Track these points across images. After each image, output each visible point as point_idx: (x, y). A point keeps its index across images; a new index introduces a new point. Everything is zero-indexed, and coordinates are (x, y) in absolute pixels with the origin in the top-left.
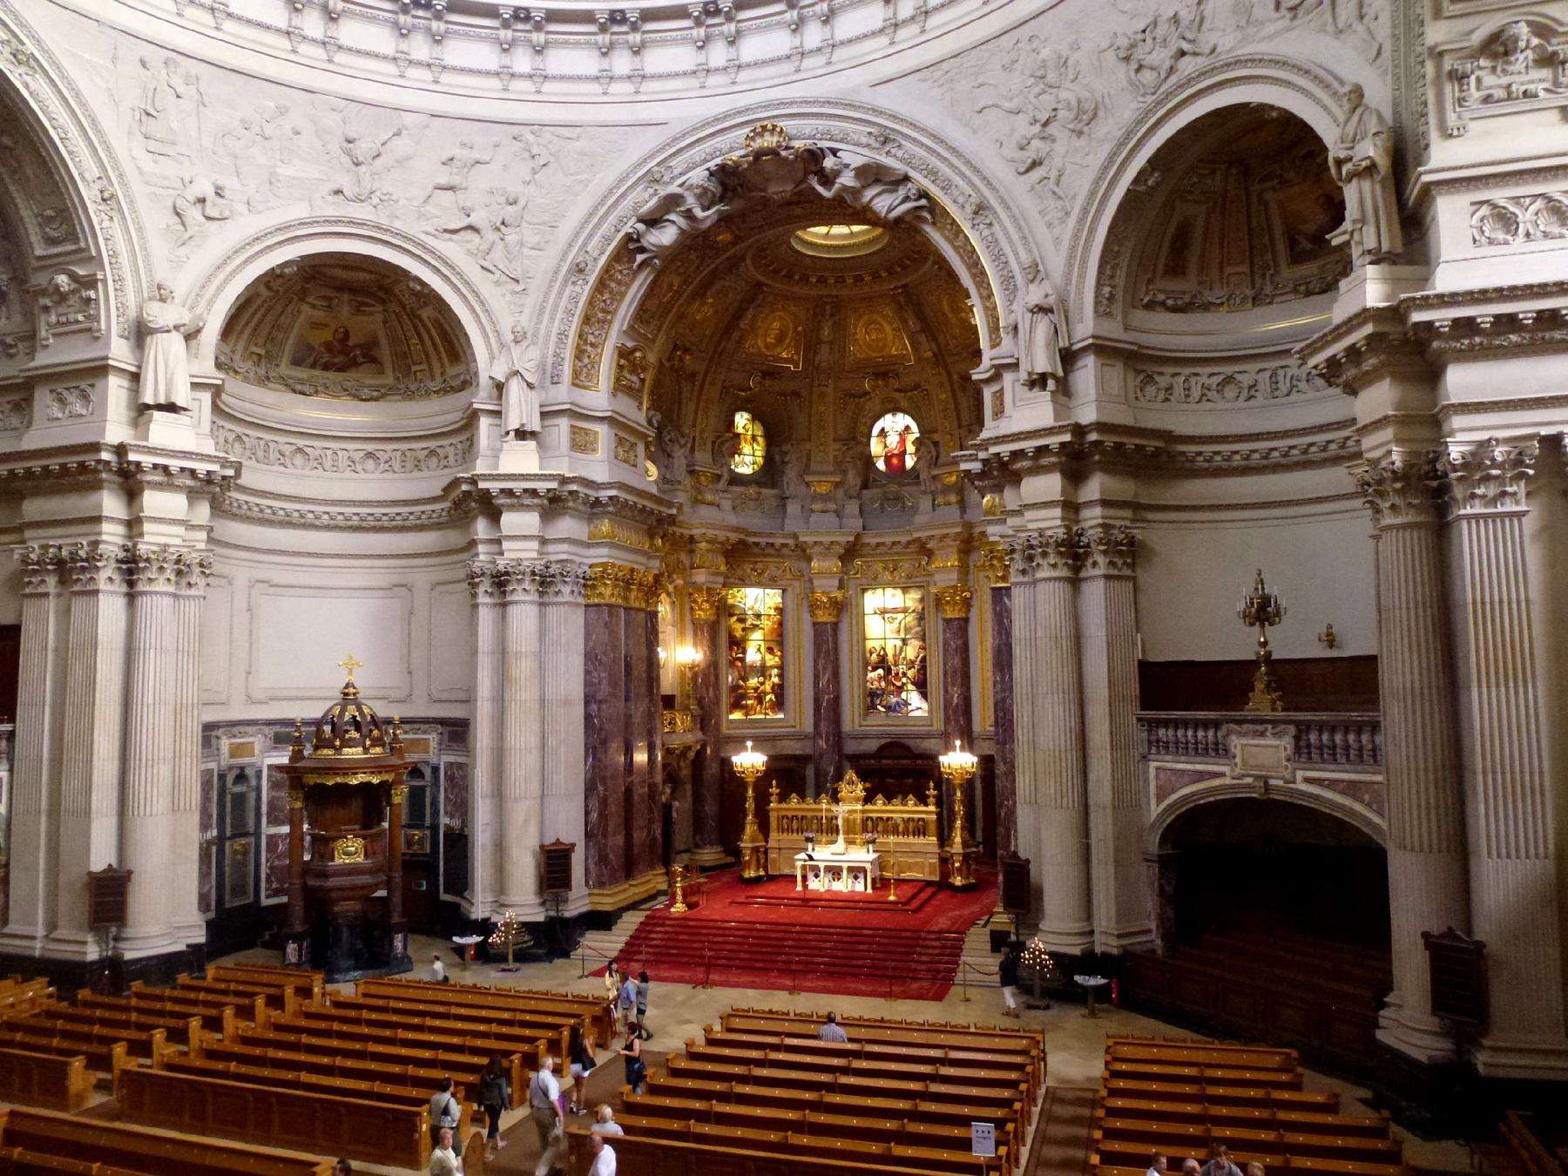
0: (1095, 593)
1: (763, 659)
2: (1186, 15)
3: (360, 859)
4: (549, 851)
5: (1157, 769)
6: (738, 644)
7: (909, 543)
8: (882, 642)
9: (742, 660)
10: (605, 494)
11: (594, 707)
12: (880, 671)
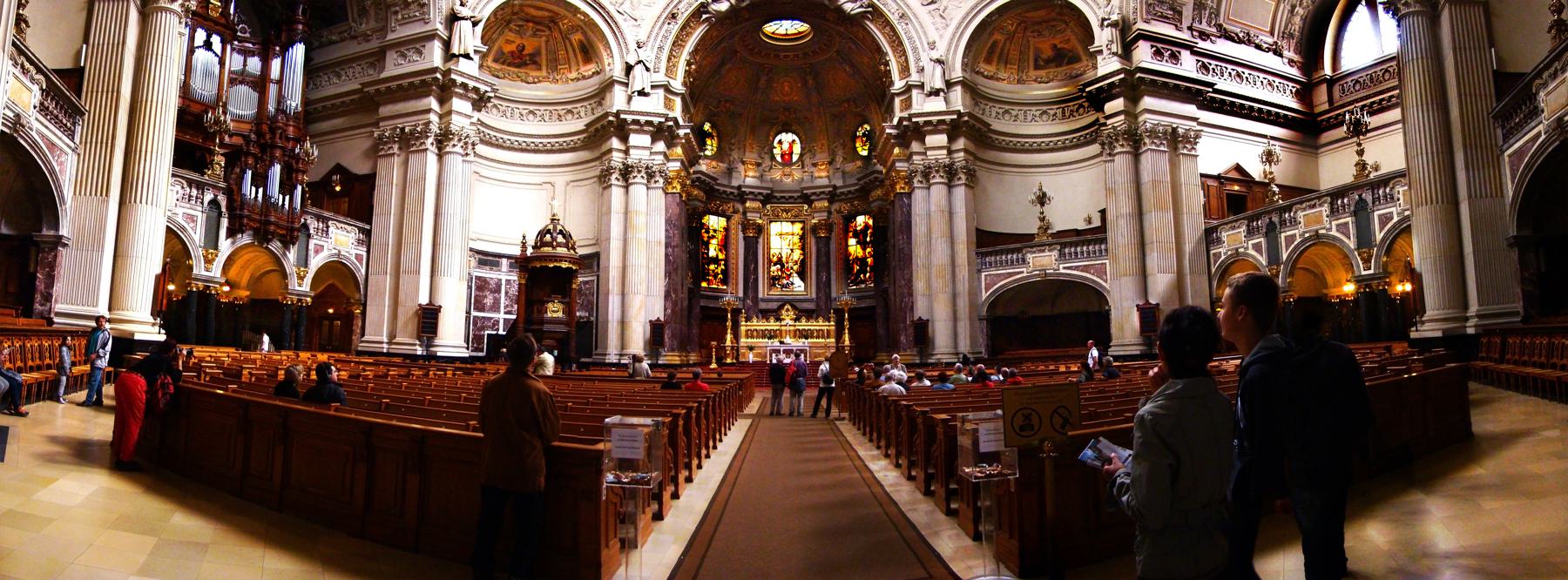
0: (960, 193)
1: (717, 256)
3: (560, 314)
4: (654, 324)
5: (986, 275)
6: (707, 244)
7: (798, 197)
8: (780, 251)
9: (708, 254)
10: (681, 132)
12: (779, 266)
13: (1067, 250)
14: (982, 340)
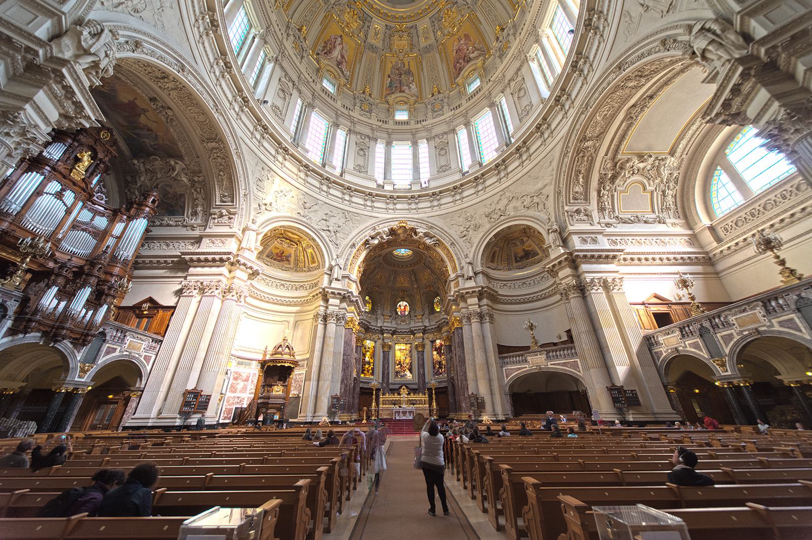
0: (487, 326)
2: (502, 209)
3: (281, 393)
6: (364, 355)
11: (345, 357)
13: (551, 354)
14: (508, 407)
